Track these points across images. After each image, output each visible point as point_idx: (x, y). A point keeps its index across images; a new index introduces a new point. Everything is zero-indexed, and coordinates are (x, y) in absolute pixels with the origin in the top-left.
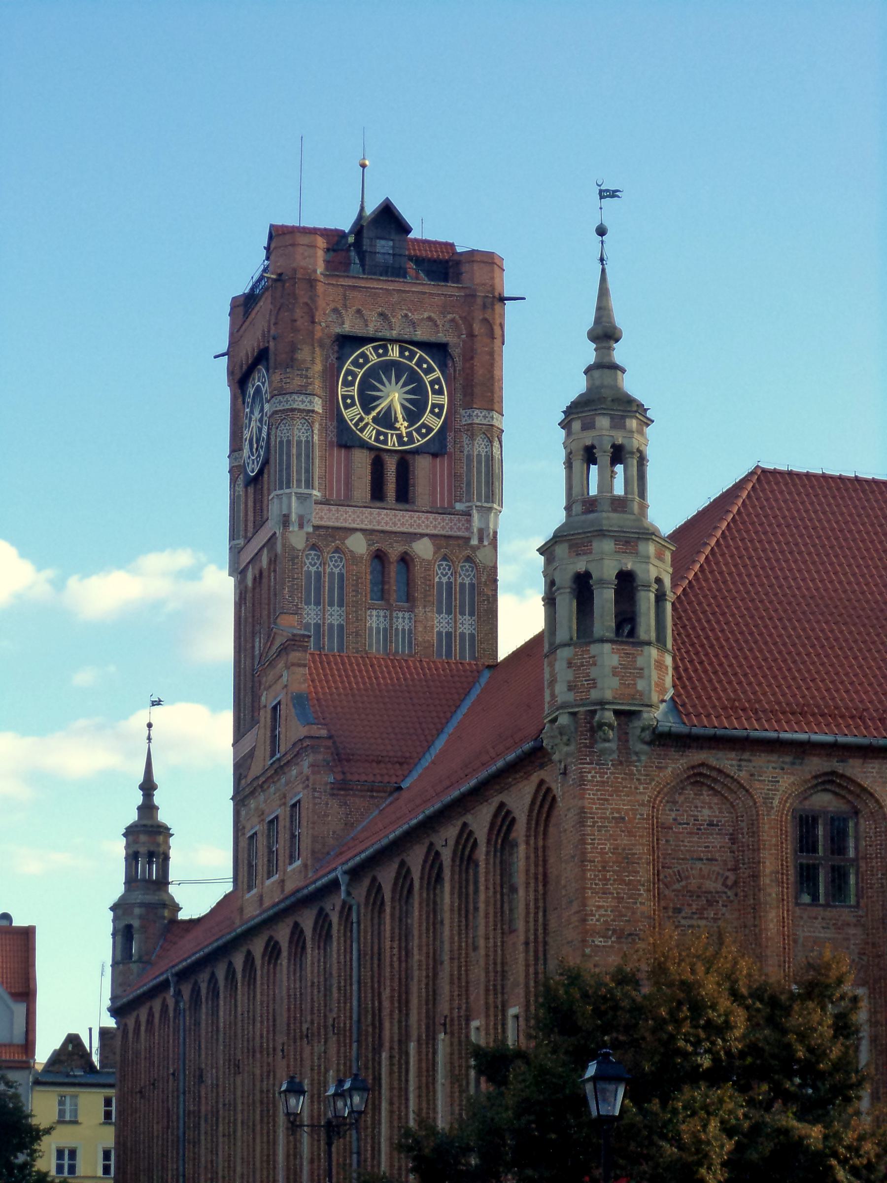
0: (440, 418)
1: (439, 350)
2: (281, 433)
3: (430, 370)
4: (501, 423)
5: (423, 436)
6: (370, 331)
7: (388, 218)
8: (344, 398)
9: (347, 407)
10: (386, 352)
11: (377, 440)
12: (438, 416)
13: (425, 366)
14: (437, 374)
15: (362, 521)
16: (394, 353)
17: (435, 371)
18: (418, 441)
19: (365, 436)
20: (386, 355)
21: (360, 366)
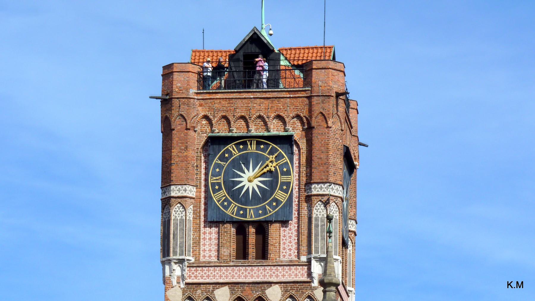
5: (274, 208)
6: (235, 133)
10: (245, 148)
12: (286, 191)
14: (286, 159)
15: (221, 276)
16: (252, 148)
18: (270, 212)
19: (229, 212)
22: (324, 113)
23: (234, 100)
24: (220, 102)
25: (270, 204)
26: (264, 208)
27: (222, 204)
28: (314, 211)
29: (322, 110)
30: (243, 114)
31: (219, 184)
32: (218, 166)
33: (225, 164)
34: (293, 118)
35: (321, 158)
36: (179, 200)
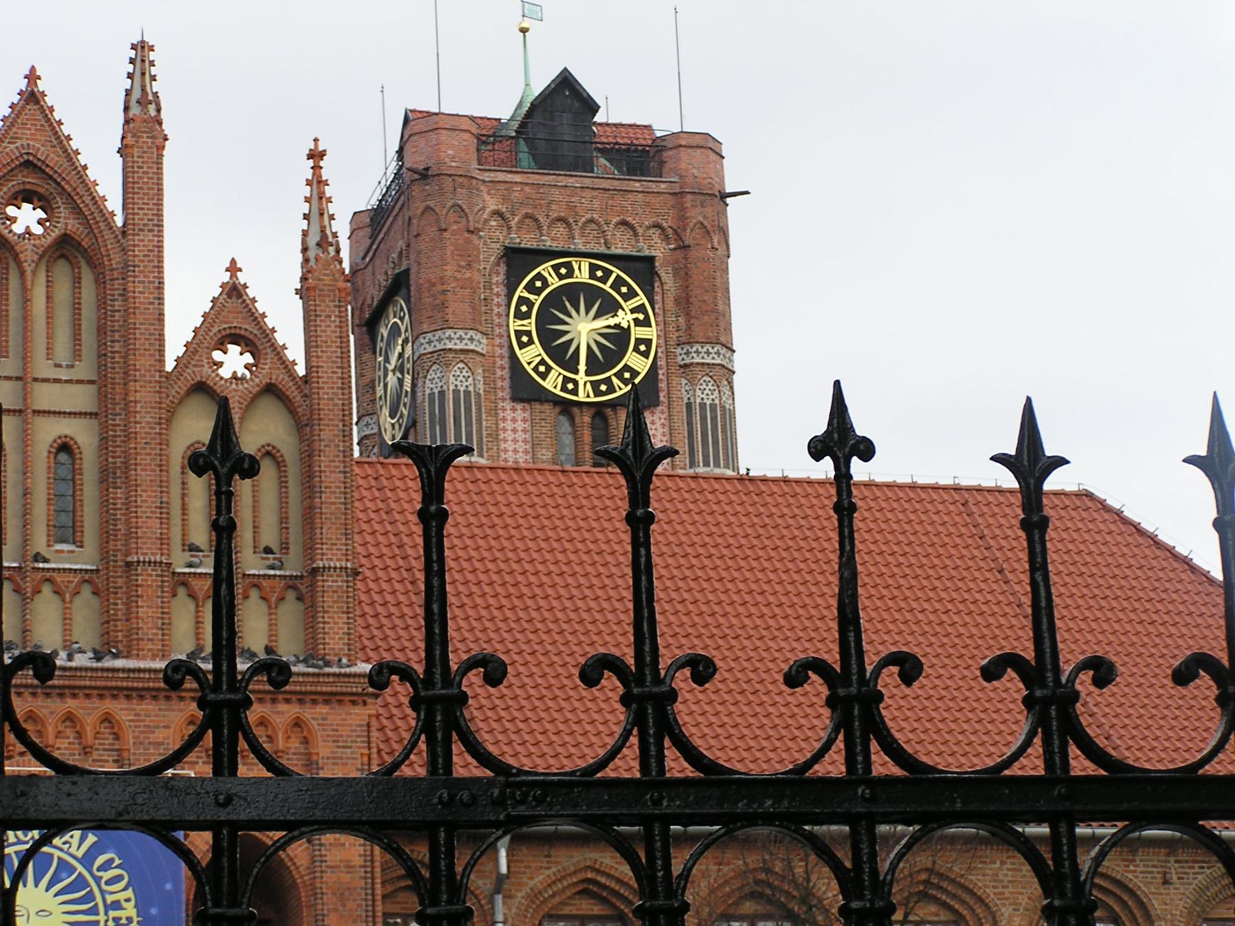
0: (647, 358)
1: (642, 269)
2: (431, 383)
3: (631, 294)
4: (731, 360)
7: (566, 99)
8: (519, 334)
9: (522, 346)
10: (570, 274)
11: (564, 389)
12: (645, 354)
13: (624, 290)
14: (642, 299)
17: (637, 295)
19: (548, 384)
20: (572, 277)
21: (537, 292)
22: (705, 223)
23: (546, 189)
24: (522, 190)
25: (619, 375)
26: (607, 381)
27: (535, 369)
28: (699, 393)
29: (701, 218)
30: (563, 214)
31: (528, 333)
32: (522, 300)
33: (537, 300)
34: (648, 228)
35: (704, 301)
36: (462, 357)
